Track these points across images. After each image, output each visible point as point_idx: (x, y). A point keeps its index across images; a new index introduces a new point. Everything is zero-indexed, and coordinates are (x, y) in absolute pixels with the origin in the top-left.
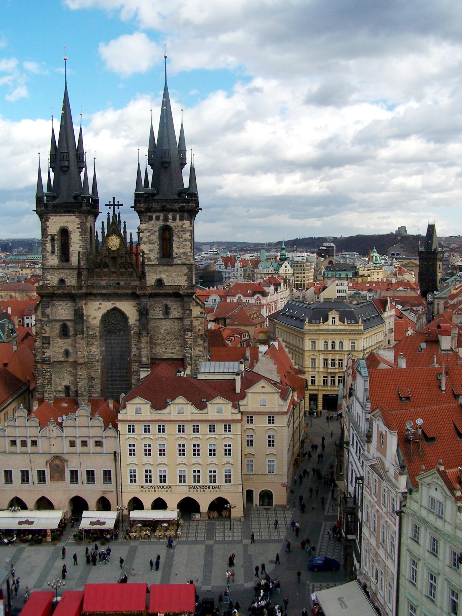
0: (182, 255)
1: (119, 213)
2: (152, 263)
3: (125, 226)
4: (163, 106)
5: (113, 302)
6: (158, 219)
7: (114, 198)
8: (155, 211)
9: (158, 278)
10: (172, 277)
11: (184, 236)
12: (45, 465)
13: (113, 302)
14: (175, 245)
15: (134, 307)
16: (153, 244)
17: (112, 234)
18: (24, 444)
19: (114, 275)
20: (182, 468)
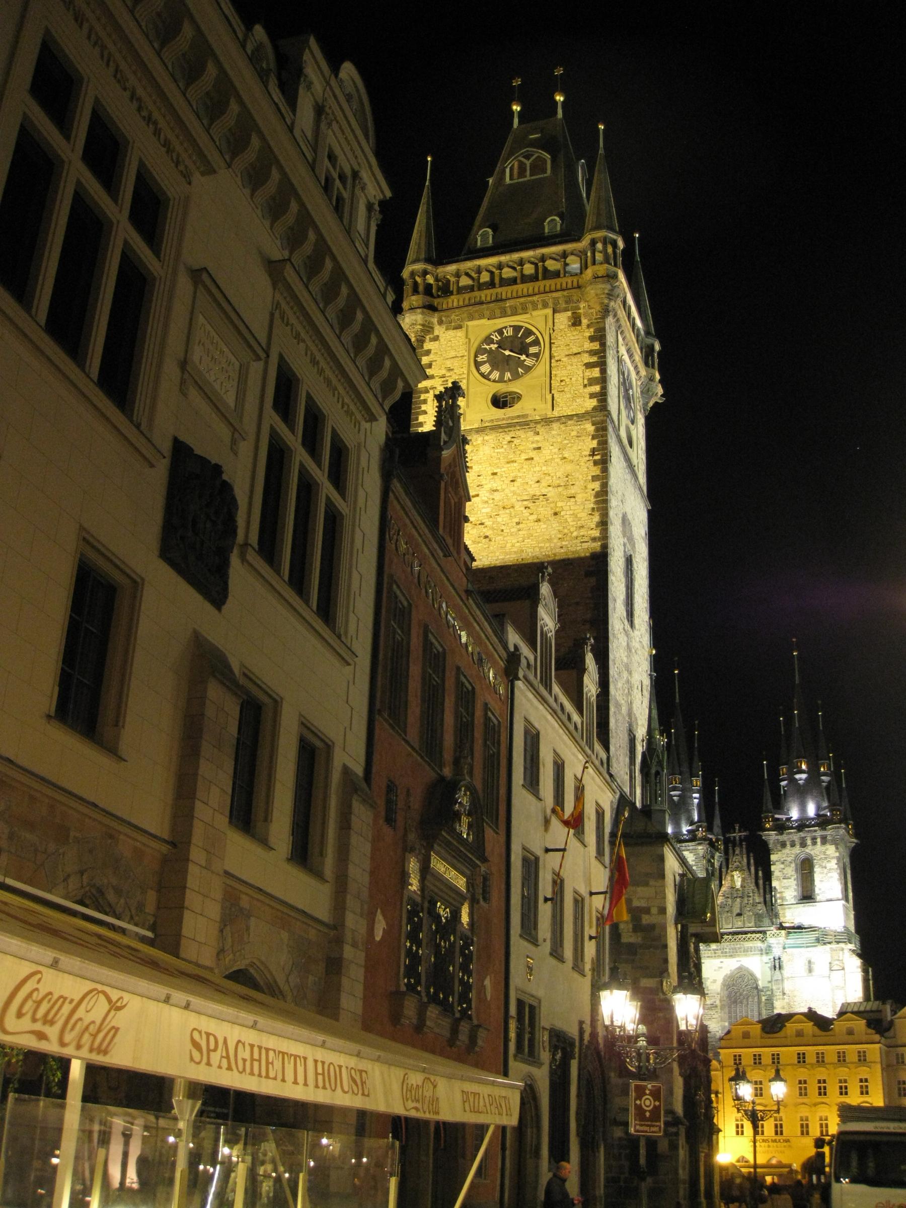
5: (738, 959)
6: (793, 845)
20: (804, 1112)
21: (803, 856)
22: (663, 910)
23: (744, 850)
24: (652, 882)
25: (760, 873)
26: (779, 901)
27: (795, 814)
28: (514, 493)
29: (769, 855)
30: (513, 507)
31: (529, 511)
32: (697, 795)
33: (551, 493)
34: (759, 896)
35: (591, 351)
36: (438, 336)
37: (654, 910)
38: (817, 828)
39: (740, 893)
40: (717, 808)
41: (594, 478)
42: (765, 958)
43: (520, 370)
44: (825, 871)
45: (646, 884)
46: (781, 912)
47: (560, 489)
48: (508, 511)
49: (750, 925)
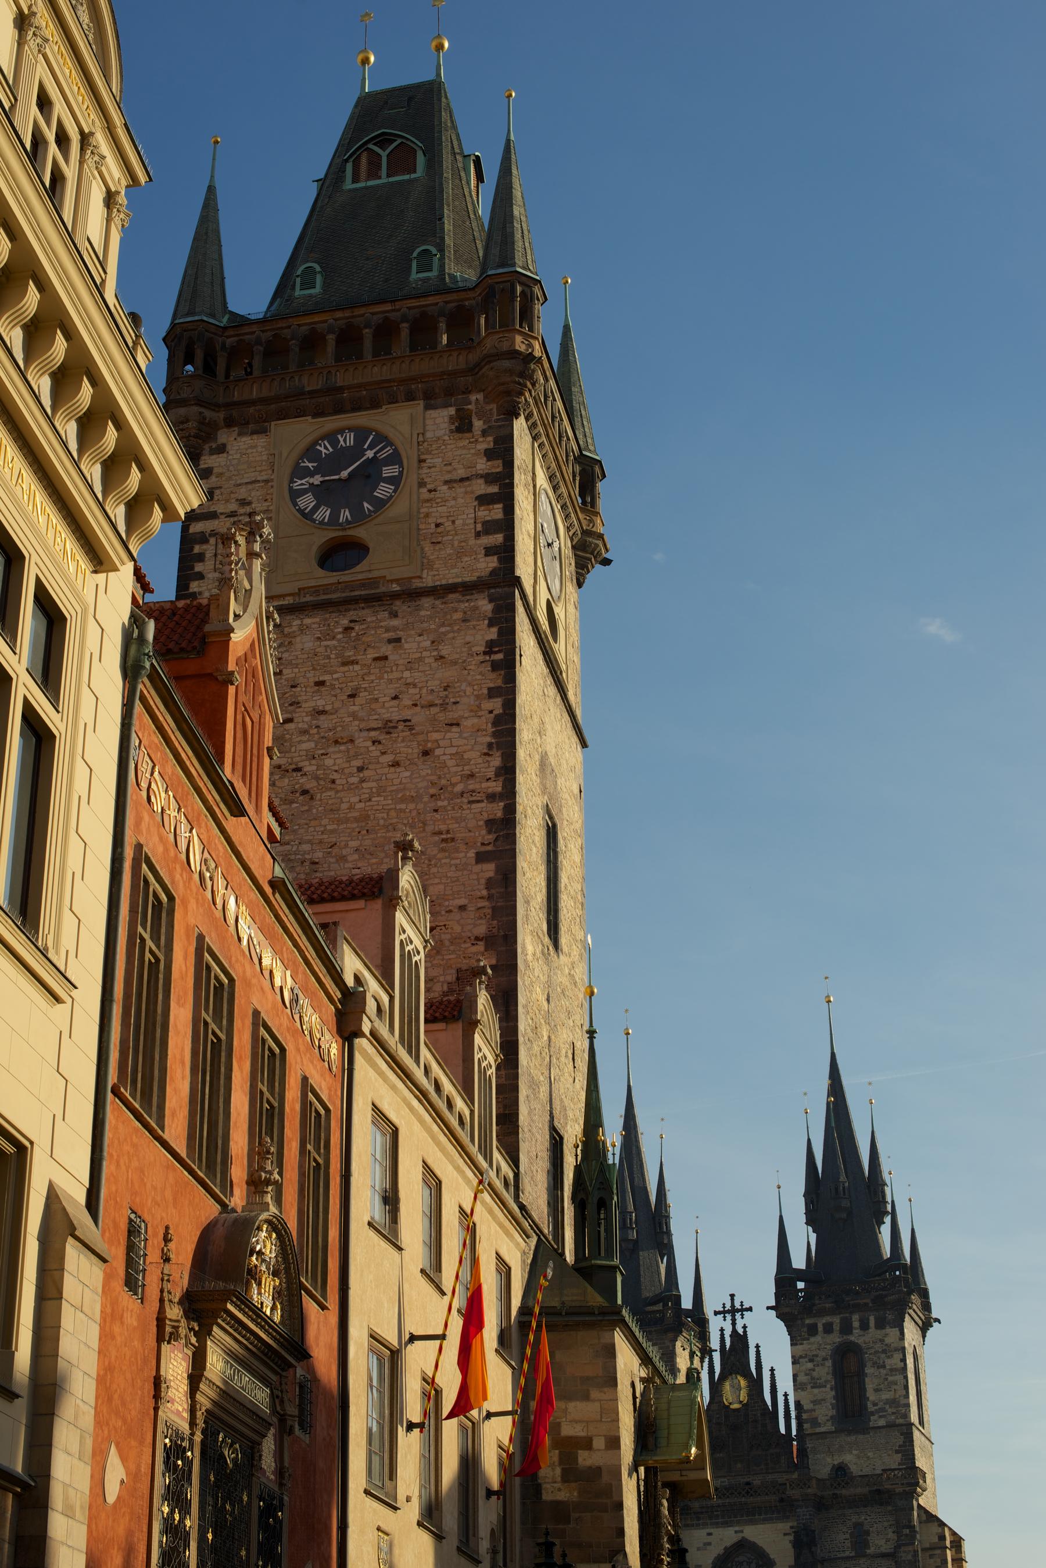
1: (745, 1327)
2: (822, 1429)
3: (758, 1353)
4: (828, 1096)
5: (737, 1528)
6: (828, 1329)
7: (732, 1296)
8: (822, 1313)
9: (836, 1463)
10: (868, 1458)
11: (888, 1362)
13: (737, 1528)
14: (870, 1385)
15: (785, 1534)
16: (820, 1387)
17: (731, 1374)
19: (739, 1465)
22: (614, 1443)
24: (595, 1394)
26: (806, 1426)
28: (354, 716)
30: (352, 741)
31: (380, 747)
33: (419, 717)
35: (488, 474)
36: (224, 446)
37: (599, 1443)
41: (492, 693)
42: (785, 1526)
43: (366, 505)
44: (883, 1371)
45: (586, 1397)
47: (434, 710)
48: (343, 748)
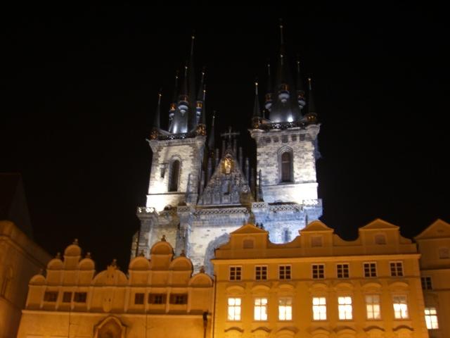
0: (304, 176)
5: (223, 228)
6: (276, 140)
11: (306, 157)
12: (92, 333)
18: (67, 297)
19: (227, 201)
21: (284, 150)
23: (235, 146)
25: (247, 162)
26: (263, 183)
27: (278, 121)
29: (256, 148)
32: (199, 113)
34: (245, 179)
38: (299, 128)
39: (228, 177)
40: (213, 128)
44: (303, 160)
46: (264, 192)
49: (236, 202)
